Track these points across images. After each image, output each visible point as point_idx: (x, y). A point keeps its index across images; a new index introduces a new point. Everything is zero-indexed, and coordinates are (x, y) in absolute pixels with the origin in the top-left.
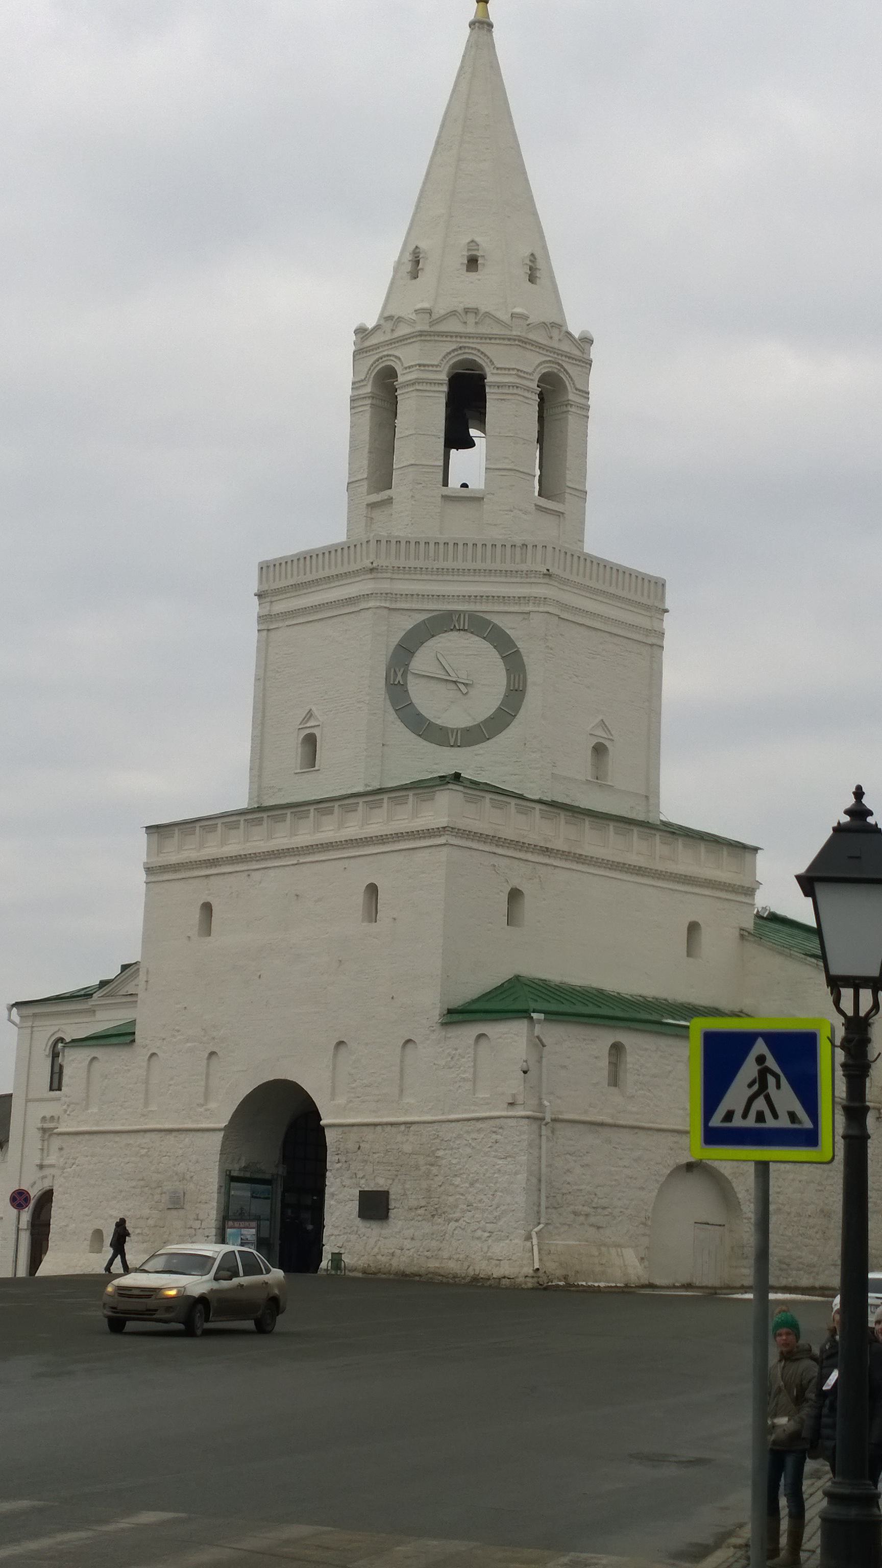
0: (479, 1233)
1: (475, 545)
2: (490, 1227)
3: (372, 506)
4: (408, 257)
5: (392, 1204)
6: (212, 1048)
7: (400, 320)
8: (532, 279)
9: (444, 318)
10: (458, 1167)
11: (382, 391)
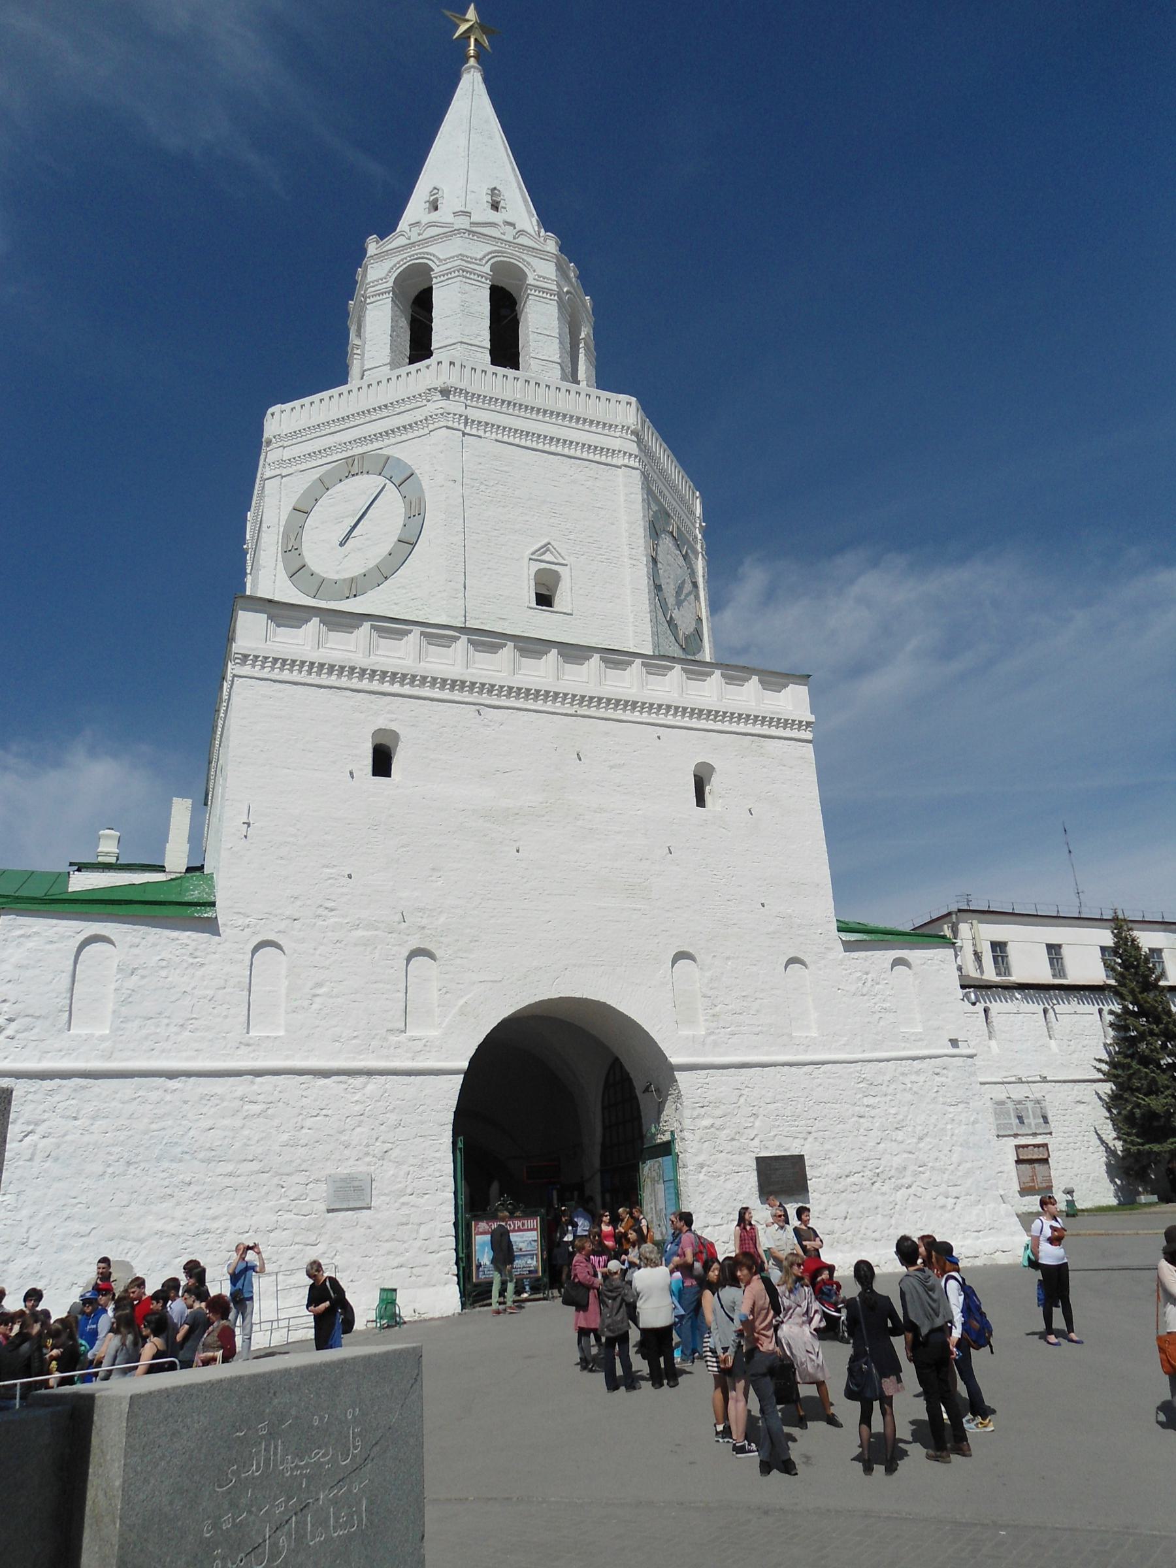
0: (941, 1200)
2: (953, 1191)
5: (809, 1173)
6: (414, 943)
7: (522, 232)
10: (900, 1117)
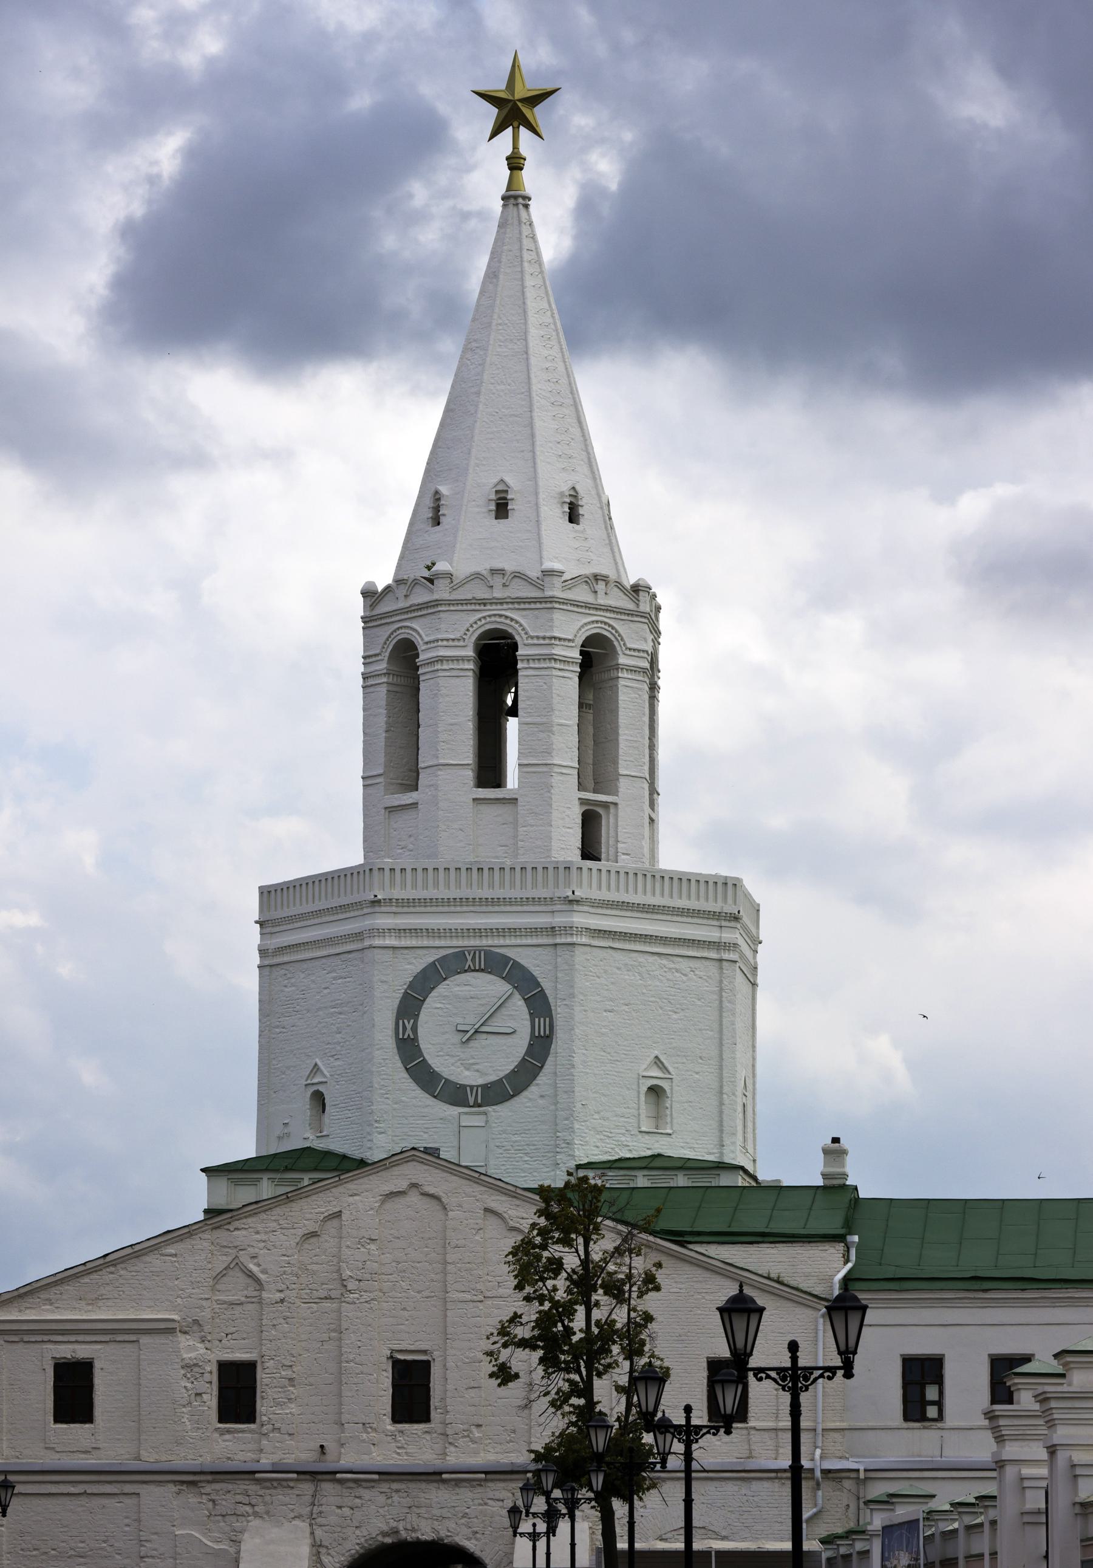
1: (491, 869)
3: (391, 810)
4: (429, 502)
8: (573, 517)
9: (462, 584)
11: (398, 669)
